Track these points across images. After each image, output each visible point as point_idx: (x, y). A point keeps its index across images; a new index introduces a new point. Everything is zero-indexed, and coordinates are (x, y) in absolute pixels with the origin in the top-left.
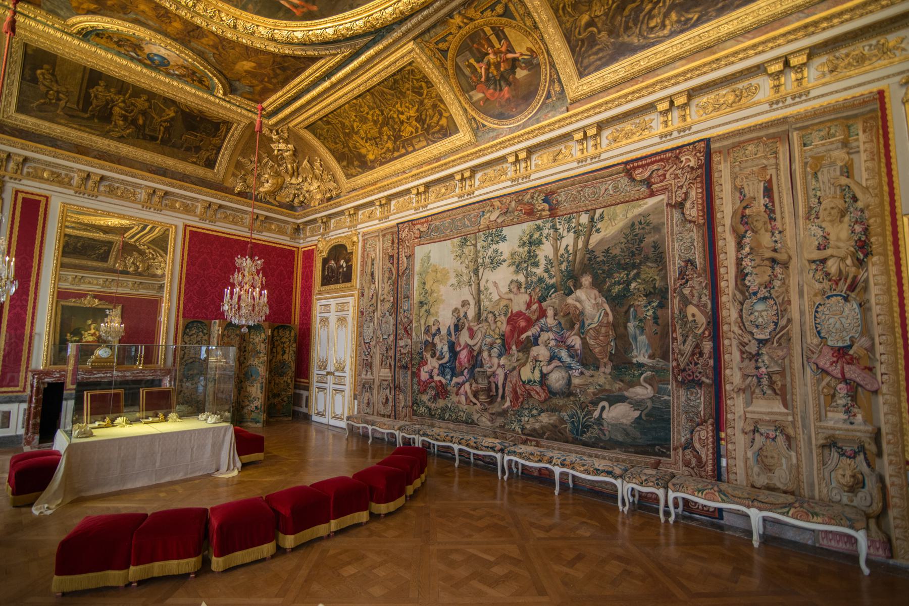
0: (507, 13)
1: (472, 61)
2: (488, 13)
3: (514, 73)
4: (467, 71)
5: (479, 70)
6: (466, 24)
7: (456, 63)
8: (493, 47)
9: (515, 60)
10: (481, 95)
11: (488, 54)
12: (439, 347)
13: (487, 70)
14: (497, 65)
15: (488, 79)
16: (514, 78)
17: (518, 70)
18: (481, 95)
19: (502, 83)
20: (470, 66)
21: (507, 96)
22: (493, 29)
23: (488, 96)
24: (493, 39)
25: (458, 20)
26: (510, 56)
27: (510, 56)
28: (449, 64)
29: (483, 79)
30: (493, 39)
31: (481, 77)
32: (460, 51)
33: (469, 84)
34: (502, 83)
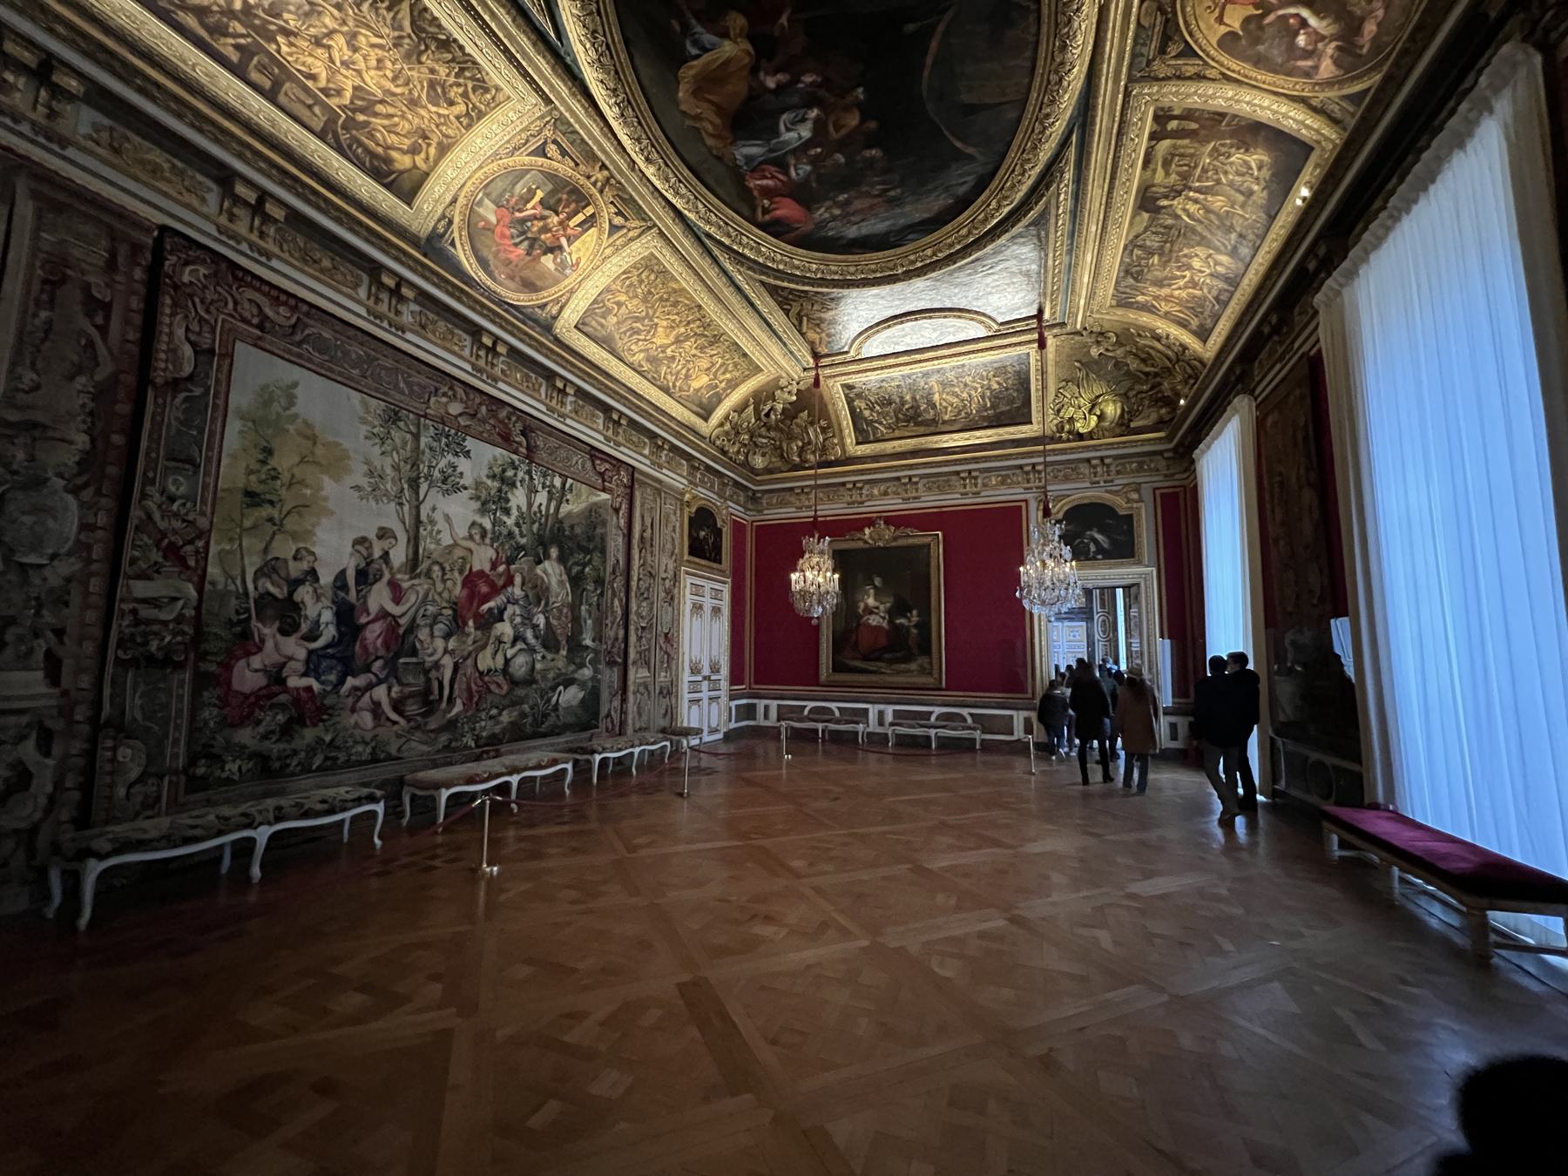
0: (614, 228)
1: (540, 194)
2: (613, 210)
3: (545, 253)
4: (520, 189)
5: (529, 206)
6: (594, 184)
7: (528, 171)
8: (569, 218)
9: (560, 248)
10: (493, 219)
11: (557, 214)
12: (311, 610)
13: (535, 217)
14: (545, 229)
15: (523, 221)
16: (539, 256)
17: (550, 256)
18: (493, 219)
19: (526, 243)
20: (532, 193)
21: (512, 256)
22: (593, 215)
23: (498, 230)
24: (580, 218)
25: (600, 176)
26: (564, 241)
27: (564, 241)
28: (522, 159)
29: (518, 215)
30: (580, 218)
31: (520, 211)
32: (551, 177)
33: (501, 195)
34: (526, 243)
